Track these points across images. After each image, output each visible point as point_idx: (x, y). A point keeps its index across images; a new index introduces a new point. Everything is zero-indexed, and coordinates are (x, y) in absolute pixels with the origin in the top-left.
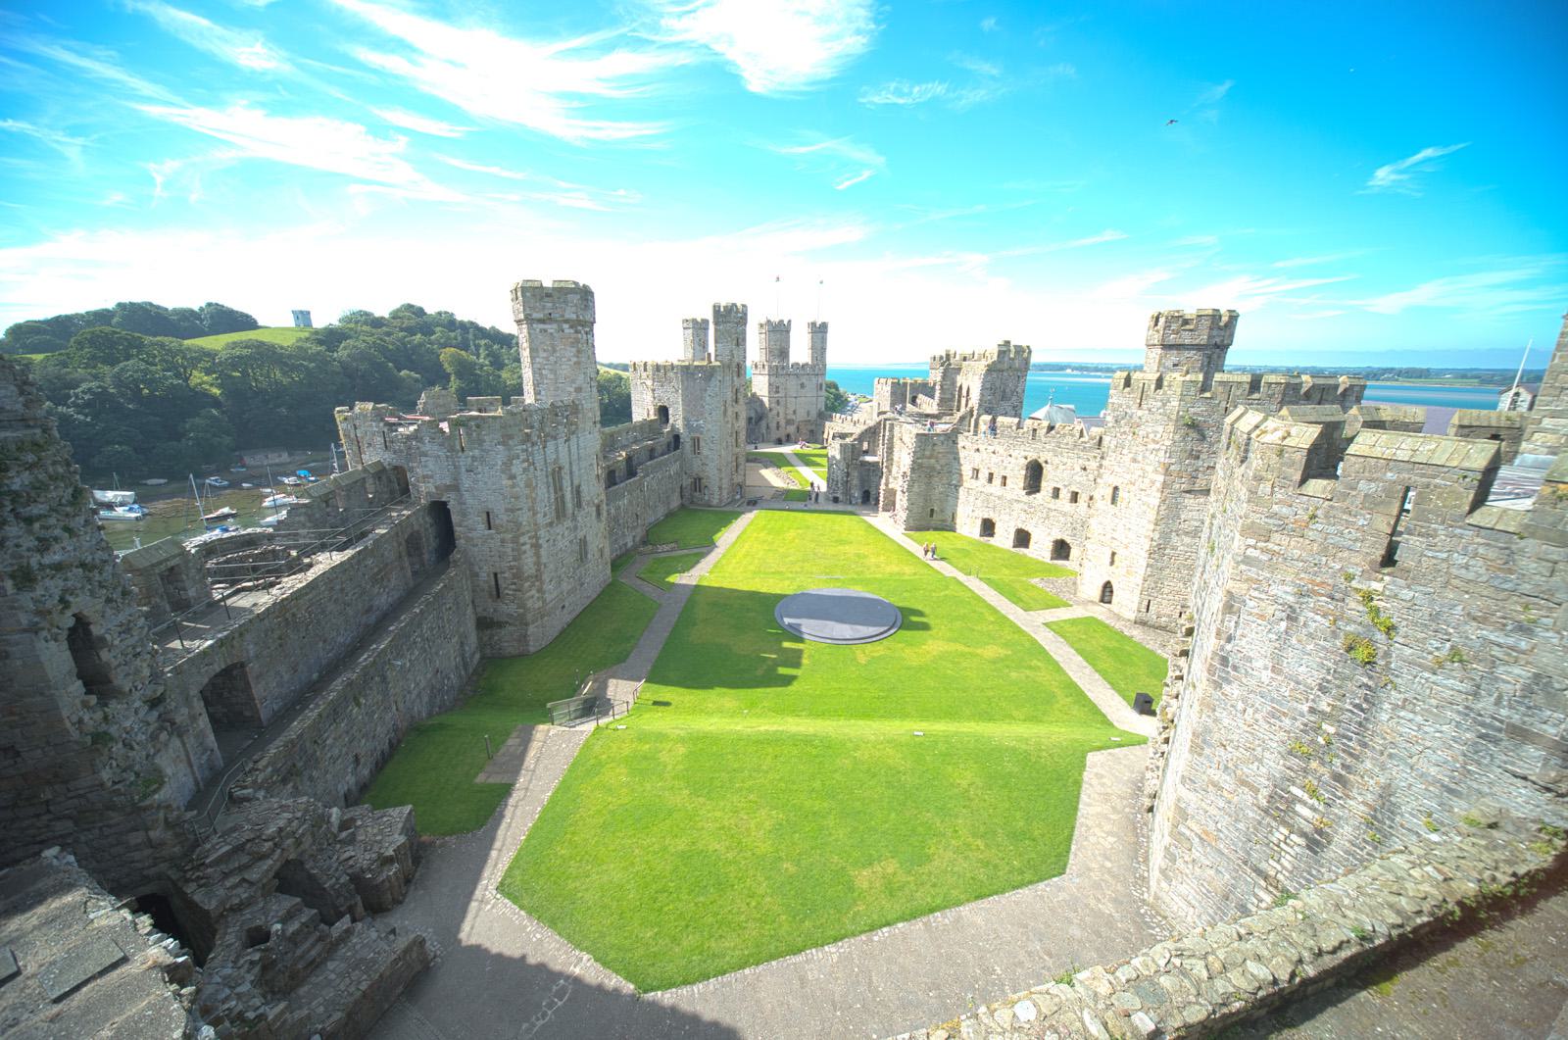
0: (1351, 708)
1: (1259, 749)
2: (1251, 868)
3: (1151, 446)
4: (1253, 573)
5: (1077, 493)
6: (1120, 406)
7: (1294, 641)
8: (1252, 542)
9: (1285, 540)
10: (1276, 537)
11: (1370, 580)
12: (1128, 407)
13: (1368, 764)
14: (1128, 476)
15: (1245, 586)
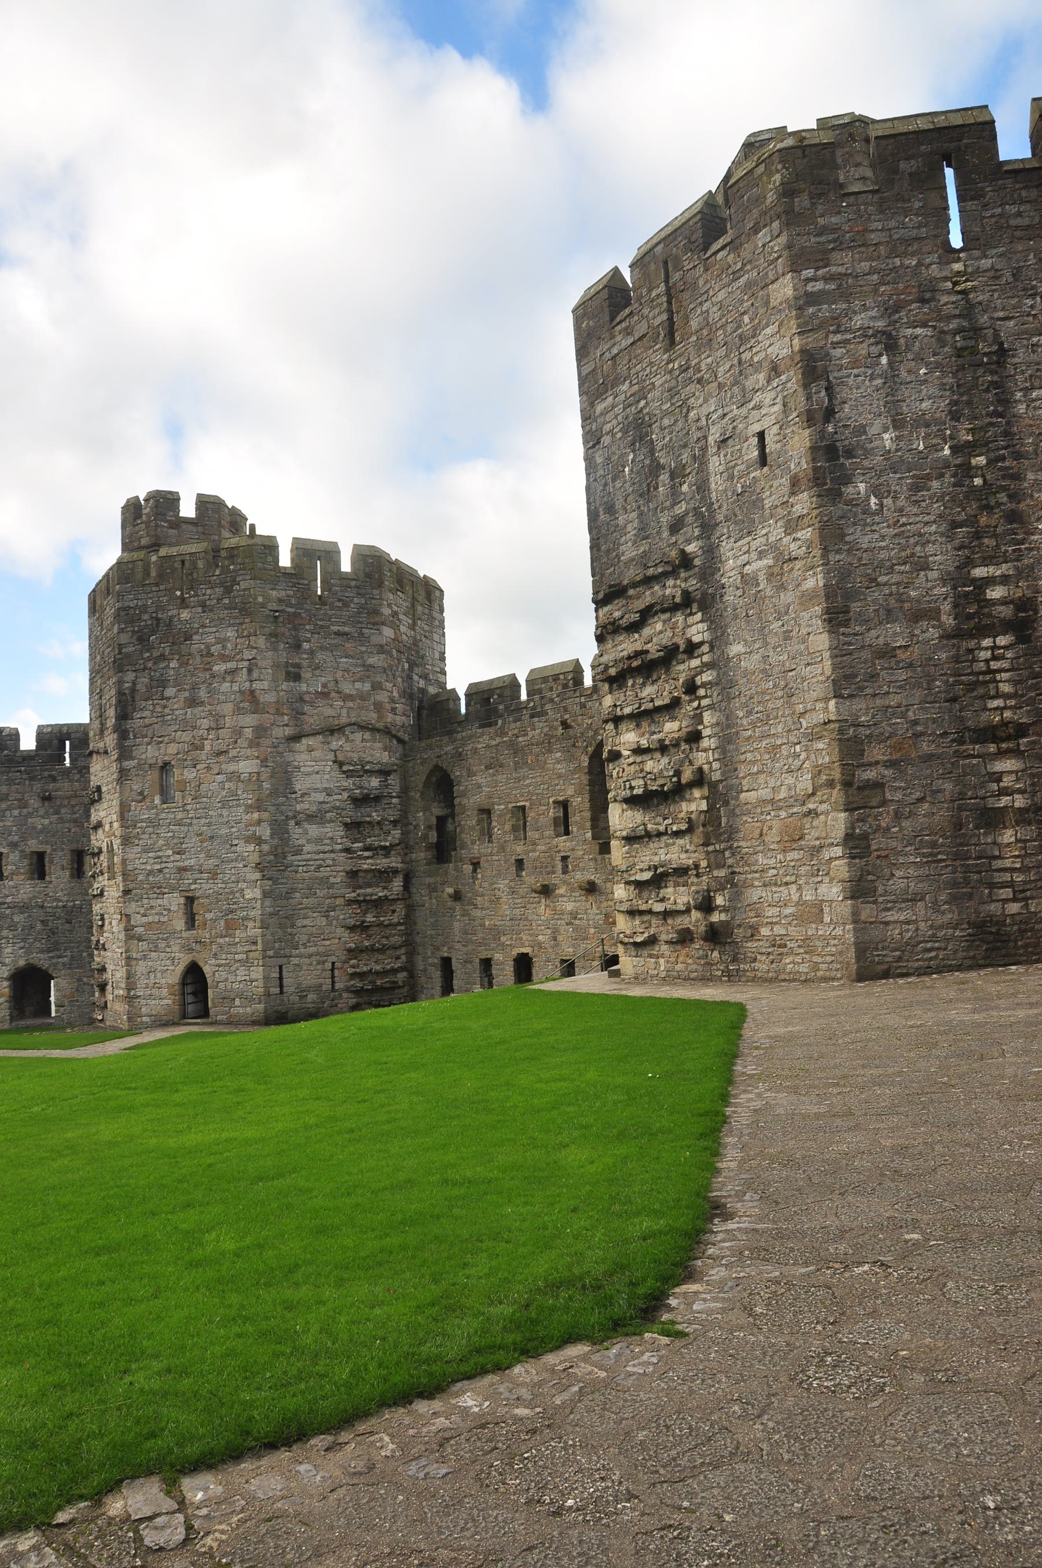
0: (988, 420)
1: (918, 548)
2: (974, 742)
3: (219, 668)
4: (825, 311)
5: (41, 856)
6: (144, 609)
7: (904, 374)
8: (809, 273)
9: (847, 257)
10: (836, 256)
11: (948, 263)
12: (160, 608)
13: (1031, 476)
14: (186, 737)
15: (821, 335)
